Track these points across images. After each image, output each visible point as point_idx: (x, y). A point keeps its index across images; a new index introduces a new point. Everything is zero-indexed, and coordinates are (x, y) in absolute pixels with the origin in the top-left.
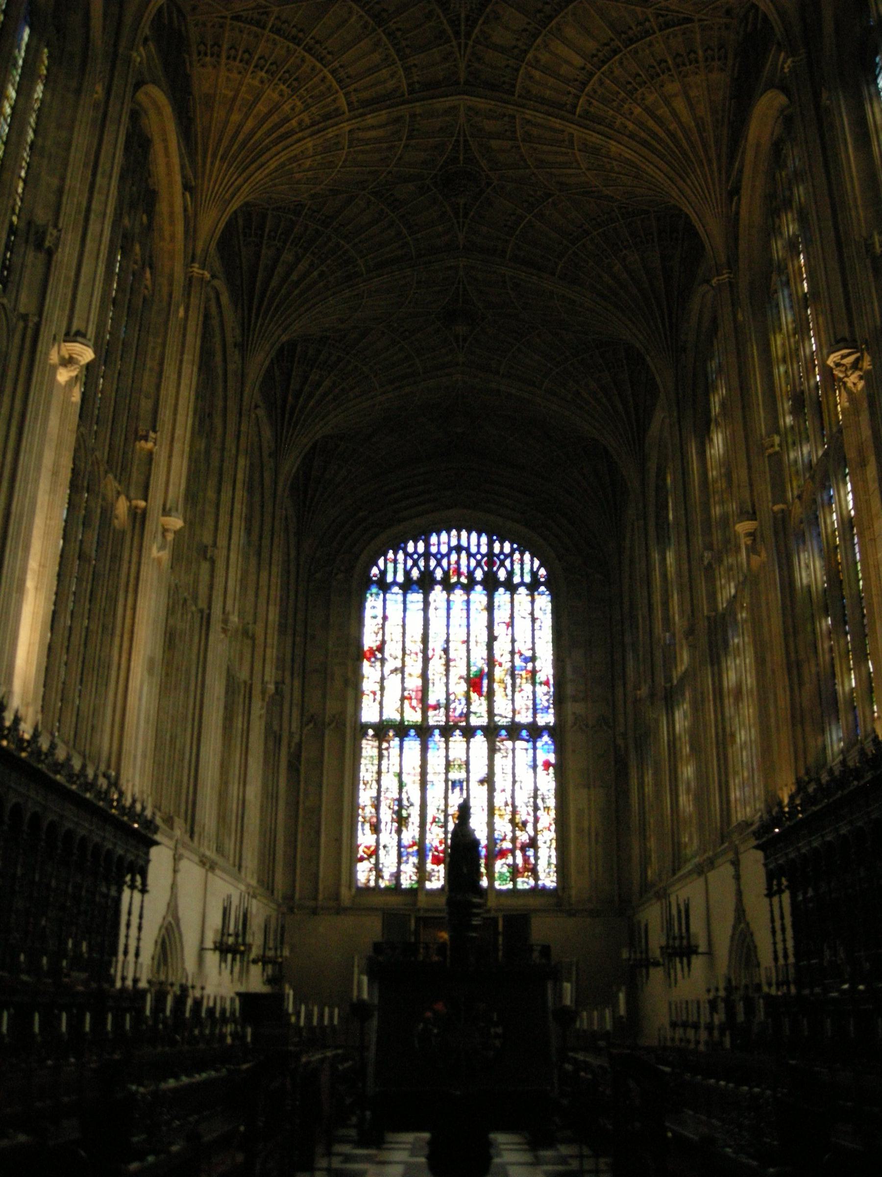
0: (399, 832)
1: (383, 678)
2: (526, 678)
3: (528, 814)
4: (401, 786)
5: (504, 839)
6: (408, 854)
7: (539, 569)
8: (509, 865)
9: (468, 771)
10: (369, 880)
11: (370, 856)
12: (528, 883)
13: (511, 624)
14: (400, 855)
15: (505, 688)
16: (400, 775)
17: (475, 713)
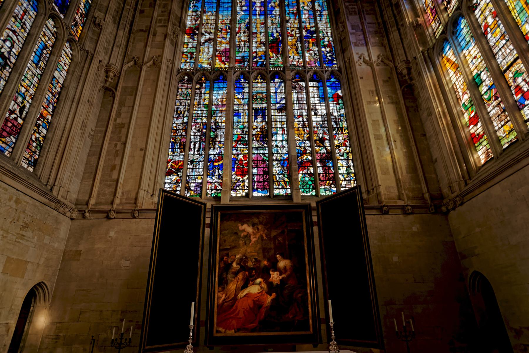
0: (206, 149)
1: (199, 44)
2: (313, 43)
3: (324, 133)
4: (210, 114)
5: (305, 153)
6: (215, 167)
8: (311, 175)
9: (269, 103)
11: (178, 170)
12: (330, 190)
13: (298, 13)
14: (207, 168)
15: (297, 49)
16: (208, 107)
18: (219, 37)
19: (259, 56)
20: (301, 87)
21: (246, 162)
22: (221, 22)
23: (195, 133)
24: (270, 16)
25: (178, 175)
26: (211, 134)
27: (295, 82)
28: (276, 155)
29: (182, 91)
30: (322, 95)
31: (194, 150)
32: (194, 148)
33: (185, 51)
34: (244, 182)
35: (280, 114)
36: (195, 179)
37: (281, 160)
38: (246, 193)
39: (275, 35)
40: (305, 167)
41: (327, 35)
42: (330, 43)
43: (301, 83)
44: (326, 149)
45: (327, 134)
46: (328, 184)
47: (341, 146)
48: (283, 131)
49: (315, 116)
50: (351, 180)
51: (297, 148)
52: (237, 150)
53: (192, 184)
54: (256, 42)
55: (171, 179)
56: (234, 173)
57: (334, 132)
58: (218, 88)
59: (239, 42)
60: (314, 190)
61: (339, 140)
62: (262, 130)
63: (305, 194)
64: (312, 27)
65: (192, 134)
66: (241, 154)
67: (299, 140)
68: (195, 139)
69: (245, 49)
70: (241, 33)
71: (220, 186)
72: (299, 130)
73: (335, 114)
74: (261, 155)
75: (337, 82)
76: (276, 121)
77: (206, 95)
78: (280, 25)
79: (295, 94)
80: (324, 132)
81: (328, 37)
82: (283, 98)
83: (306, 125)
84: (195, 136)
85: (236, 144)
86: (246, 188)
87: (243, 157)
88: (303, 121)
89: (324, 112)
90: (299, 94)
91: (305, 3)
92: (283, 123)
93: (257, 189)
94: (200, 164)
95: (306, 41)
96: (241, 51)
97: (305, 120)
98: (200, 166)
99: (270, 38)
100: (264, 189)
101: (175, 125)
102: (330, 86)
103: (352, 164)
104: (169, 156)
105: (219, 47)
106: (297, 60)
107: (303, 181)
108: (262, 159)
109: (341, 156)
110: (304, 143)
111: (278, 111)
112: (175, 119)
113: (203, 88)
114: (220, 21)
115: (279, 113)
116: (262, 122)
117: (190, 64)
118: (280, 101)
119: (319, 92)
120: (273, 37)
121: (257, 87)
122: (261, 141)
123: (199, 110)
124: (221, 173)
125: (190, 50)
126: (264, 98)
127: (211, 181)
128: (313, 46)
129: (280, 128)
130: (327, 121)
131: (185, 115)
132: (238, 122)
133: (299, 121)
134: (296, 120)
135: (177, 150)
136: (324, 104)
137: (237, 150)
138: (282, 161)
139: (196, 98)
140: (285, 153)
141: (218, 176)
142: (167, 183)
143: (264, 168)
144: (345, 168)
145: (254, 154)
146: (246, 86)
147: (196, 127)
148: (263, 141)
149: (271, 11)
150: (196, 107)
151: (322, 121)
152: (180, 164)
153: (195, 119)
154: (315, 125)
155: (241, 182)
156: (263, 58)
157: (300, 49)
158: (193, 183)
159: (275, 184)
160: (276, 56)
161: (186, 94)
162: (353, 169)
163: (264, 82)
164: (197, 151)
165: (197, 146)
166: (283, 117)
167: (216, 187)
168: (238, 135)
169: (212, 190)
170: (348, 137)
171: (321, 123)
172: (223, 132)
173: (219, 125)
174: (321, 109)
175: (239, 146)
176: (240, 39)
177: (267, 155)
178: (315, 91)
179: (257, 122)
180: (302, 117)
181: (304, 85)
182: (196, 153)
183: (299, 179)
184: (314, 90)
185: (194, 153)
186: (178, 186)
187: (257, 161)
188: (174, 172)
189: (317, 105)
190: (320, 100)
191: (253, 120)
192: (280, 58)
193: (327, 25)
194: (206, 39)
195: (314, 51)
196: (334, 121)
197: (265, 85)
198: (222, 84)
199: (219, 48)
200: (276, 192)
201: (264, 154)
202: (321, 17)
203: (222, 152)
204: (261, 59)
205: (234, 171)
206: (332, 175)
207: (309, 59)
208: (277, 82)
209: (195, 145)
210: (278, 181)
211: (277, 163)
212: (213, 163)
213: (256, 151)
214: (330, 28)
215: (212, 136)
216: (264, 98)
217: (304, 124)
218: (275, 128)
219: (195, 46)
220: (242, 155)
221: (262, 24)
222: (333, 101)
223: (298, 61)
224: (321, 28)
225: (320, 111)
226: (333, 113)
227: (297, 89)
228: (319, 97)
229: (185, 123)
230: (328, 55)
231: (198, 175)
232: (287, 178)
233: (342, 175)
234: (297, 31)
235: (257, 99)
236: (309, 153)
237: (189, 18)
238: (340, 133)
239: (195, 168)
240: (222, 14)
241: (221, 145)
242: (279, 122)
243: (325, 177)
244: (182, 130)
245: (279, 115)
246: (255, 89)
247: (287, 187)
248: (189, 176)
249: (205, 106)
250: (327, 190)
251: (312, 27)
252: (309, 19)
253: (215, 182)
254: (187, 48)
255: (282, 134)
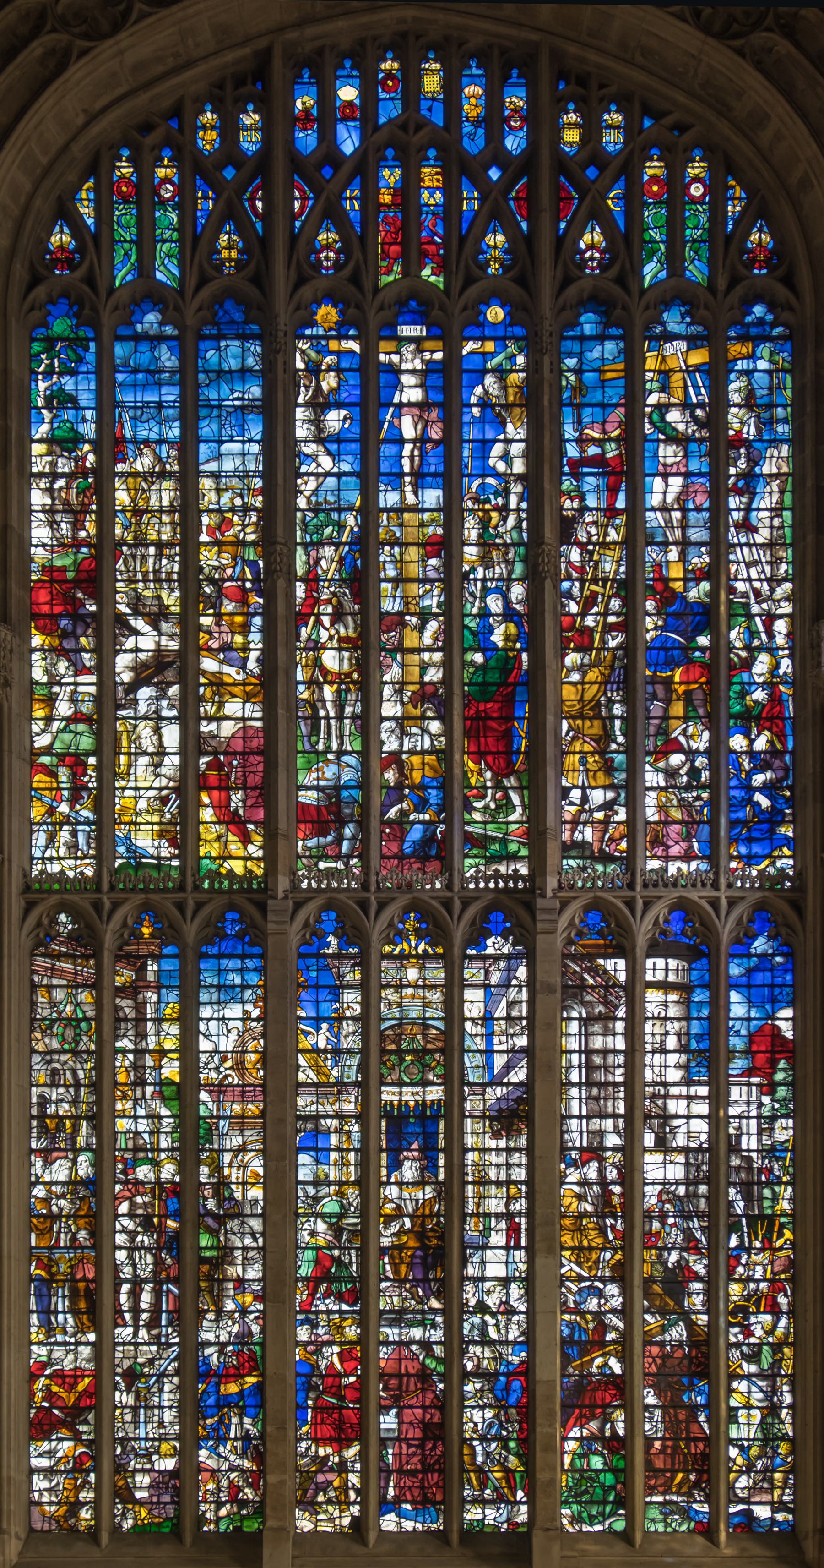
3: (690, 1245)
7: (744, 223)
10: (75, 1506)
11: (75, 1414)
12: (686, 1514)
17: (481, 842)
18: (209, 649)
19: (412, 787)
20: (609, 984)
21: (352, 1379)
22: (211, 531)
23: (132, 1235)
24: (477, 483)
25: (77, 1437)
26: (203, 1243)
27: (583, 957)
28: (478, 1350)
29: (53, 1004)
30: (699, 1037)
31: (136, 1319)
32: (136, 1311)
33: (41, 742)
34: (347, 1471)
35: (502, 1144)
36: (148, 1456)
37: (497, 1374)
38: (353, 1517)
39: (497, 638)
40: (592, 1407)
41: (771, 635)
42: (775, 698)
43: (609, 964)
44: (691, 1326)
45: (697, 1251)
46: (680, 1485)
47: (753, 1309)
48: (513, 1230)
49: (659, 1157)
50: (774, 1471)
51: (567, 1317)
52: (314, 1325)
53: (139, 1478)
54: (400, 686)
55: (51, 1453)
56: (304, 1429)
57: (734, 1242)
58: (219, 987)
59: (311, 683)
60: (622, 1512)
61: (750, 1279)
62: (423, 1225)
63: (586, 1528)
64: (698, 576)
65: (121, 1239)
66: (330, 1343)
67: (580, 1279)
68: (134, 1266)
69: (341, 737)
70: (318, 622)
71: (250, 1485)
72: (580, 1229)
73: (750, 1142)
74: (414, 1348)
75: (778, 959)
76: (482, 1182)
77: (165, 1026)
78: (525, 560)
79: (574, 1027)
80: (688, 1234)
81: (772, 650)
82: (522, 1050)
83: (616, 1200)
84: (132, 1249)
85: (312, 1295)
86: (352, 1495)
87: (340, 1355)
88: (603, 1181)
89: (701, 1127)
90: (597, 1028)
91: (677, 379)
92: (513, 1190)
93: (398, 1501)
94: (167, 1388)
95: (653, 681)
96: (321, 747)
97: (612, 1174)
98: (166, 1396)
99: (468, 657)
100: (423, 1503)
101: (39, 1192)
102: (746, 986)
103: (788, 1399)
104: (34, 1348)
105: (210, 719)
106: (599, 815)
107: (582, 1471)
108: (417, 1366)
109: (749, 1358)
110: (600, 1294)
111: (497, 1126)
112: (39, 1163)
113: (148, 987)
114: (205, 520)
115: (496, 1135)
116: (420, 1183)
117: (74, 834)
118: (508, 1068)
119: (688, 1019)
120: (487, 648)
121: (400, 986)
122: (416, 1282)
123: (141, 1112)
124: (253, 1431)
125: (67, 737)
126: (431, 1052)
127: (212, 1463)
128: (686, 719)
129: (497, 1215)
130: (707, 1181)
131: (81, 1142)
132: (316, 1183)
133: (584, 1183)
134: (573, 1176)
135: (61, 1317)
136: (703, 1091)
137: (314, 1325)
138: (502, 1379)
139: (119, 1044)
140: (515, 1343)
141: (239, 1444)
142: (39, 1470)
143: (424, 1408)
144: (757, 1415)
145: (387, 1343)
146: (349, 977)
147: (133, 1205)
148: (425, 1280)
149: (486, 445)
150: (124, 1097)
151: (687, 1182)
152: (81, 1387)
153: (124, 1161)
154: (654, 1200)
155: (331, 1470)
156: (434, 796)
157: (621, 739)
158: (143, 1471)
159: (469, 1481)
160: (498, 786)
161: (73, 1022)
162: (789, 1420)
163: (436, 957)
164: (149, 1326)
165: (146, 1299)
166: (516, 1158)
167: (235, 1489)
168: (318, 1249)
169: (219, 1505)
170: (791, 1264)
171: (682, 1190)
172: (253, 1235)
173: (232, 1198)
174: (688, 1117)
175: (322, 1307)
176: (318, 664)
177: (438, 1350)
178: (673, 1012)
179: (400, 1184)
180: (601, 1160)
181: (622, 977)
182: (143, 1333)
183: (567, 1459)
184: (665, 1004)
185: (135, 1334)
186: (82, 1486)
187: (399, 1376)
188: (62, 1423)
189: (674, 1090)
190: (686, 1067)
191: (384, 1172)
192: (516, 799)
193: (775, 562)
194: (142, 656)
195: (691, 754)
196: (742, 1183)
197: (437, 973)
198: (238, 963)
199: (213, 726)
200: (473, 1514)
201: (426, 1345)
202: (753, 495)
203: (251, 1334)
204: (421, 805)
205: (305, 1422)
206: (701, 1445)
207: (662, 808)
208: (496, 958)
209: (135, 1295)
210: (479, 1470)
211: (478, 1386)
212: (218, 1385)
213: (396, 1331)
214: (788, 586)
215: (208, 1254)
216: (431, 1052)
217: (606, 1194)
218: (477, 1215)
219: (86, 708)
220: (336, 1349)
221: (431, 547)
222: (749, 1072)
223: (606, 822)
224: (741, 586)
225: (684, 1129)
226: (739, 1137)
227: (588, 998)
228: (683, 1049)
229: (85, 1183)
230: (759, 779)
231: (160, 1440)
232: (517, 1455)
233: (742, 1448)
234: (615, 604)
235: (400, 1053)
236: (614, 1342)
237: (38, 498)
238: (758, 1244)
239: (147, 1408)
240: (213, 467)
241: (249, 1299)
242: (498, 1184)
243: (672, 1456)
244: (76, 1217)
245: (498, 1150)
246: (390, 994)
247: (515, 1496)
248: (122, 1439)
249: (168, 1091)
250: (672, 1513)
251: (698, 576)
252: (684, 510)
253: (232, 1469)
254: (49, 719)
255: (507, 1248)
